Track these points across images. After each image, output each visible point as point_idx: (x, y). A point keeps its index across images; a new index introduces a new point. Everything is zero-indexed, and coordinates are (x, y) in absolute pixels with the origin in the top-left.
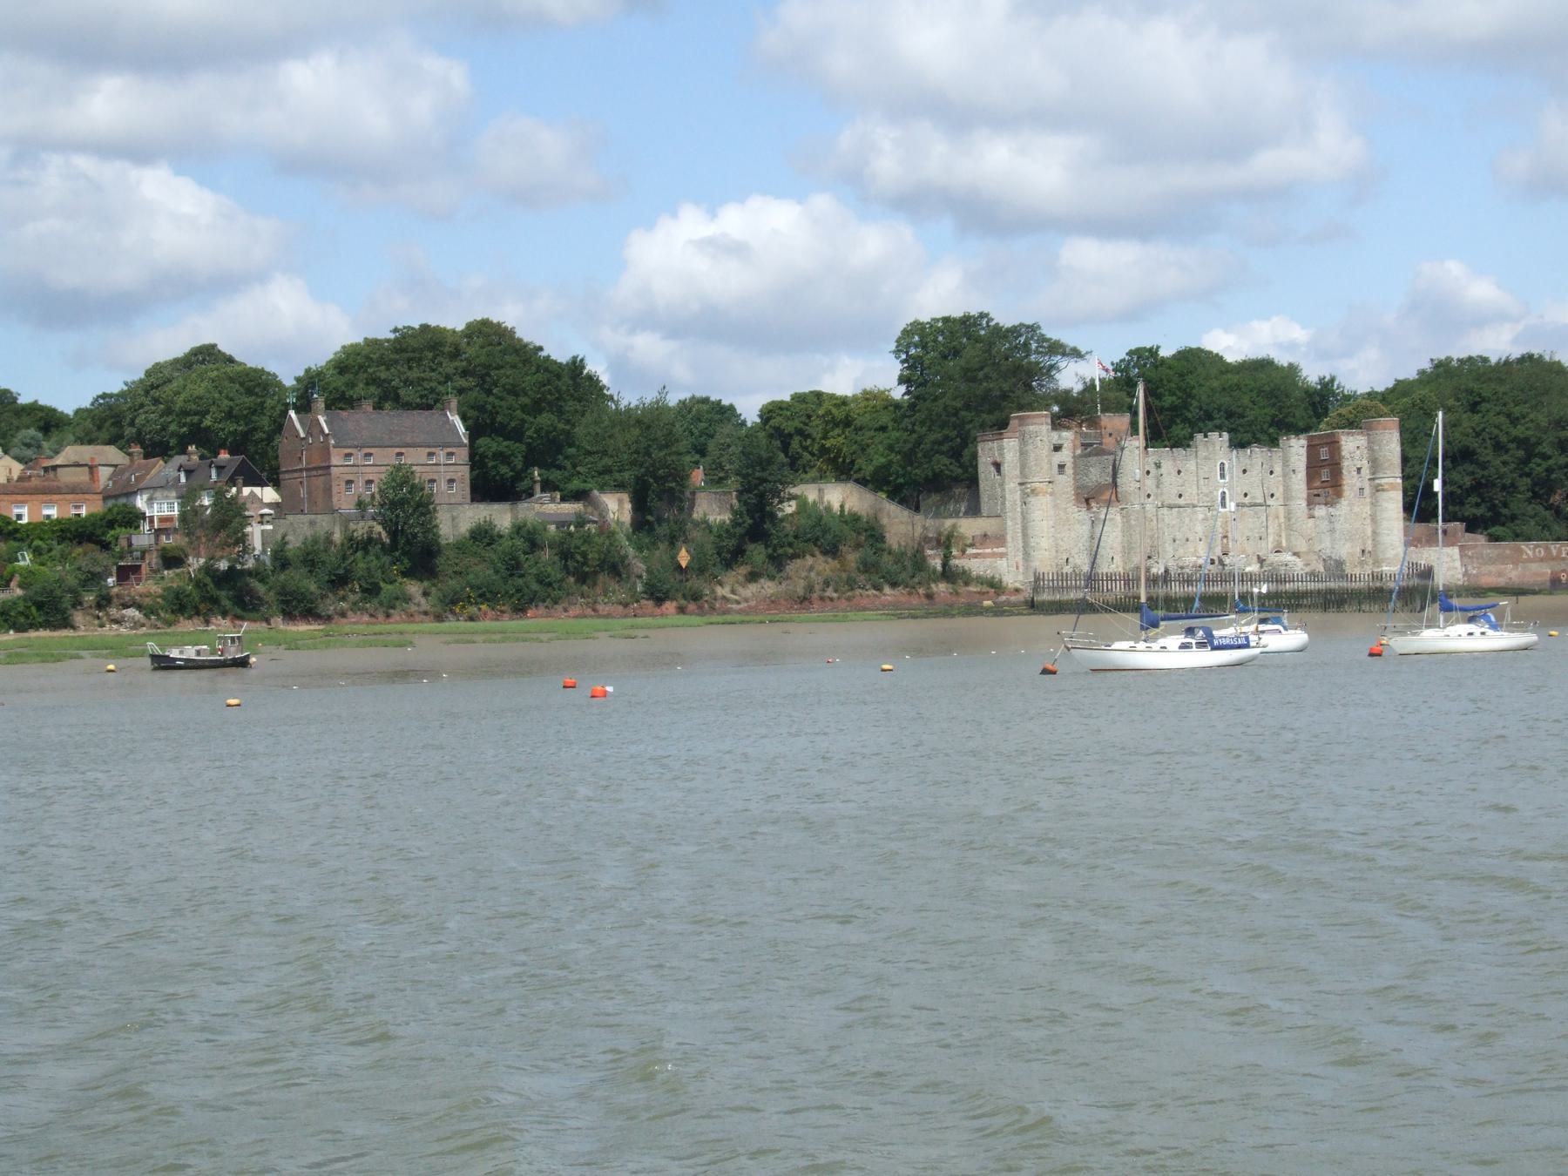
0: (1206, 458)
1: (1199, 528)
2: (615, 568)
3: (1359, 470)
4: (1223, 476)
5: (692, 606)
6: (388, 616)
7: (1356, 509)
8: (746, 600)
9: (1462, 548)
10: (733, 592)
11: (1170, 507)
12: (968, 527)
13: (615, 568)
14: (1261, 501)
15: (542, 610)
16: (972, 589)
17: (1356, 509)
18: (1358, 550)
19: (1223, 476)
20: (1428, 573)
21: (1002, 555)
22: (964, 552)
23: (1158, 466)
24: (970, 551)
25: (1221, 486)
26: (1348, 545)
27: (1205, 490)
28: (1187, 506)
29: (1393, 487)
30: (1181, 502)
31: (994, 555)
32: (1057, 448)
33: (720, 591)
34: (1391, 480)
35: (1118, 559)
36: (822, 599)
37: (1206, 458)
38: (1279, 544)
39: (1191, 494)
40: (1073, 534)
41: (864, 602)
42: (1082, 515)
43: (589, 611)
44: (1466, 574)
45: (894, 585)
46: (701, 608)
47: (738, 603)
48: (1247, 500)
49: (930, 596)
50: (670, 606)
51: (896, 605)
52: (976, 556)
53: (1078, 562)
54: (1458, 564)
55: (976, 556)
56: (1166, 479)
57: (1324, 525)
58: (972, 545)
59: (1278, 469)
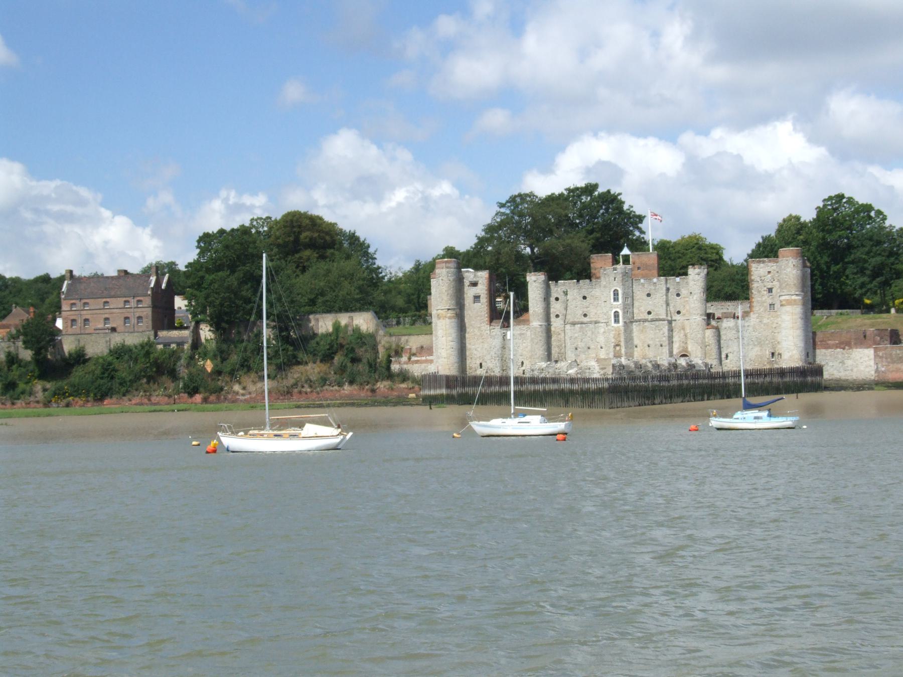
0: (605, 287)
2: (173, 374)
3: (770, 290)
4: (616, 299)
5: (213, 398)
6: (13, 404)
7: (765, 321)
8: (250, 393)
9: (876, 350)
10: (244, 388)
11: (574, 324)
12: (414, 342)
13: (173, 374)
14: (664, 317)
15: (114, 400)
16: (403, 386)
17: (765, 321)
18: (768, 353)
19: (616, 299)
20: (819, 371)
21: (431, 361)
22: (409, 359)
23: (566, 293)
24: (413, 358)
26: (757, 349)
28: (591, 322)
29: (789, 303)
30: (585, 320)
31: (427, 361)
32: (474, 284)
33: (237, 387)
34: (787, 297)
36: (300, 392)
38: (686, 349)
41: (328, 395)
43: (146, 401)
44: (877, 371)
45: (351, 383)
46: (218, 398)
47: (243, 395)
48: (650, 317)
49: (373, 391)
50: (198, 398)
51: (349, 397)
52: (417, 362)
53: (491, 365)
54: (872, 363)
55: (417, 362)
56: (572, 305)
58: (414, 355)
59: (684, 292)
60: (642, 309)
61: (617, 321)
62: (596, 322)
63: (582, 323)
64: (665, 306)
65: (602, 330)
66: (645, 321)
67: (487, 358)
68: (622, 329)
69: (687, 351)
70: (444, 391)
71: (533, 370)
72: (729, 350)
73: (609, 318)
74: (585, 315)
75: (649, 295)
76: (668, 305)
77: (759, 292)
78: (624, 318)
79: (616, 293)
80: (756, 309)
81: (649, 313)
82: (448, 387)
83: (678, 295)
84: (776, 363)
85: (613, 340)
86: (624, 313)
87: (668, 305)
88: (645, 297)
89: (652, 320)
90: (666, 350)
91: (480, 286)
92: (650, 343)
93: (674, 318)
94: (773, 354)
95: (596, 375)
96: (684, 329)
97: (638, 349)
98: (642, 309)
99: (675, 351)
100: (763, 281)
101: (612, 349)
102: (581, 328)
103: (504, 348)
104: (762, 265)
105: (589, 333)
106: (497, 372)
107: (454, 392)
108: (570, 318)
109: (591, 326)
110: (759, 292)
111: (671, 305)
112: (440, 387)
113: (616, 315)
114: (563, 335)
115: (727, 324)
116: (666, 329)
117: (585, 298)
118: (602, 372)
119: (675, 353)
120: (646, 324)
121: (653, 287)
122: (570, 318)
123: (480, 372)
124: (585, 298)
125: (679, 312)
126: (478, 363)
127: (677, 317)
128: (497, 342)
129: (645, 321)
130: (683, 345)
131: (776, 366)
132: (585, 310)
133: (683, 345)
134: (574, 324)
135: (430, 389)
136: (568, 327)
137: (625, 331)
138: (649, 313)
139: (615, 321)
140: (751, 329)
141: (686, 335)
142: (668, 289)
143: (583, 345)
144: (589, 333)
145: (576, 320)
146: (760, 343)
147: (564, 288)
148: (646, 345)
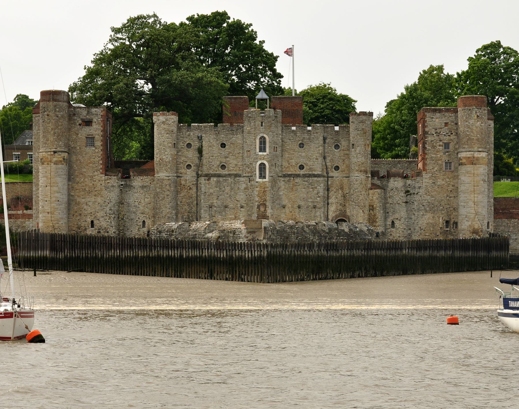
0: (249, 133)
1: (241, 197)
4: (262, 149)
7: (440, 182)
11: (208, 176)
17: (440, 182)
19: (262, 149)
21: (30, 217)
23: (200, 138)
25: (263, 157)
26: (429, 215)
27: (247, 161)
28: (230, 175)
30: (225, 172)
31: (24, 216)
32: (88, 123)
34: (468, 154)
35: (148, 222)
37: (249, 133)
39: (233, 164)
40: (99, 200)
42: (114, 181)
48: (302, 172)
53: (104, 224)
57: (399, 197)
60: (293, 162)
61: (262, 176)
62: (236, 176)
63: (219, 176)
64: (320, 159)
65: (244, 186)
66: (298, 176)
67: (100, 214)
68: (268, 185)
69: (345, 216)
70: (47, 253)
71: (160, 232)
72: (397, 216)
73: (253, 171)
74: (223, 167)
75: (301, 145)
76: (324, 158)
77: (434, 147)
78: (270, 172)
79: (263, 141)
80: (429, 167)
81: (302, 167)
82: (53, 248)
83: (337, 147)
84: (451, 234)
85: (257, 199)
86: (271, 166)
87: (324, 158)
88: (297, 148)
89: (305, 176)
90: (320, 213)
91: (95, 126)
92: (302, 203)
93: (331, 174)
94: (447, 222)
95: (242, 240)
96: (342, 188)
97: (287, 210)
98: (293, 162)
99: (331, 215)
100: (438, 134)
101: (255, 209)
102: (218, 182)
103: (121, 203)
104: (438, 115)
105: (228, 189)
106: (112, 232)
107: (61, 255)
108: (205, 170)
109: (230, 180)
110: (434, 147)
111: (328, 159)
112: (43, 249)
113: (262, 167)
114: (195, 190)
115: (396, 183)
116: (321, 188)
117: (223, 145)
118: (250, 237)
119: (330, 217)
120: (298, 180)
121: (306, 136)
122: (205, 170)
123: (91, 232)
124: (223, 145)
125: (337, 168)
126: (89, 220)
127: (334, 174)
128: (113, 195)
129: (298, 176)
130: (340, 207)
131: (451, 237)
132: (224, 160)
133: (340, 207)
134: (208, 176)
135: (29, 250)
136: (202, 180)
137: (272, 187)
138: (302, 167)
139: (260, 177)
140: (422, 191)
141: (344, 196)
142: (325, 139)
143: (219, 203)
144: (228, 189)
145: (211, 172)
146: (432, 208)
147: (197, 133)
148: (296, 206)
